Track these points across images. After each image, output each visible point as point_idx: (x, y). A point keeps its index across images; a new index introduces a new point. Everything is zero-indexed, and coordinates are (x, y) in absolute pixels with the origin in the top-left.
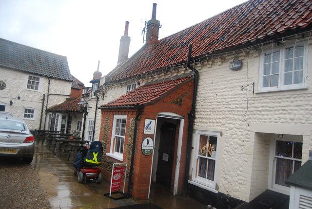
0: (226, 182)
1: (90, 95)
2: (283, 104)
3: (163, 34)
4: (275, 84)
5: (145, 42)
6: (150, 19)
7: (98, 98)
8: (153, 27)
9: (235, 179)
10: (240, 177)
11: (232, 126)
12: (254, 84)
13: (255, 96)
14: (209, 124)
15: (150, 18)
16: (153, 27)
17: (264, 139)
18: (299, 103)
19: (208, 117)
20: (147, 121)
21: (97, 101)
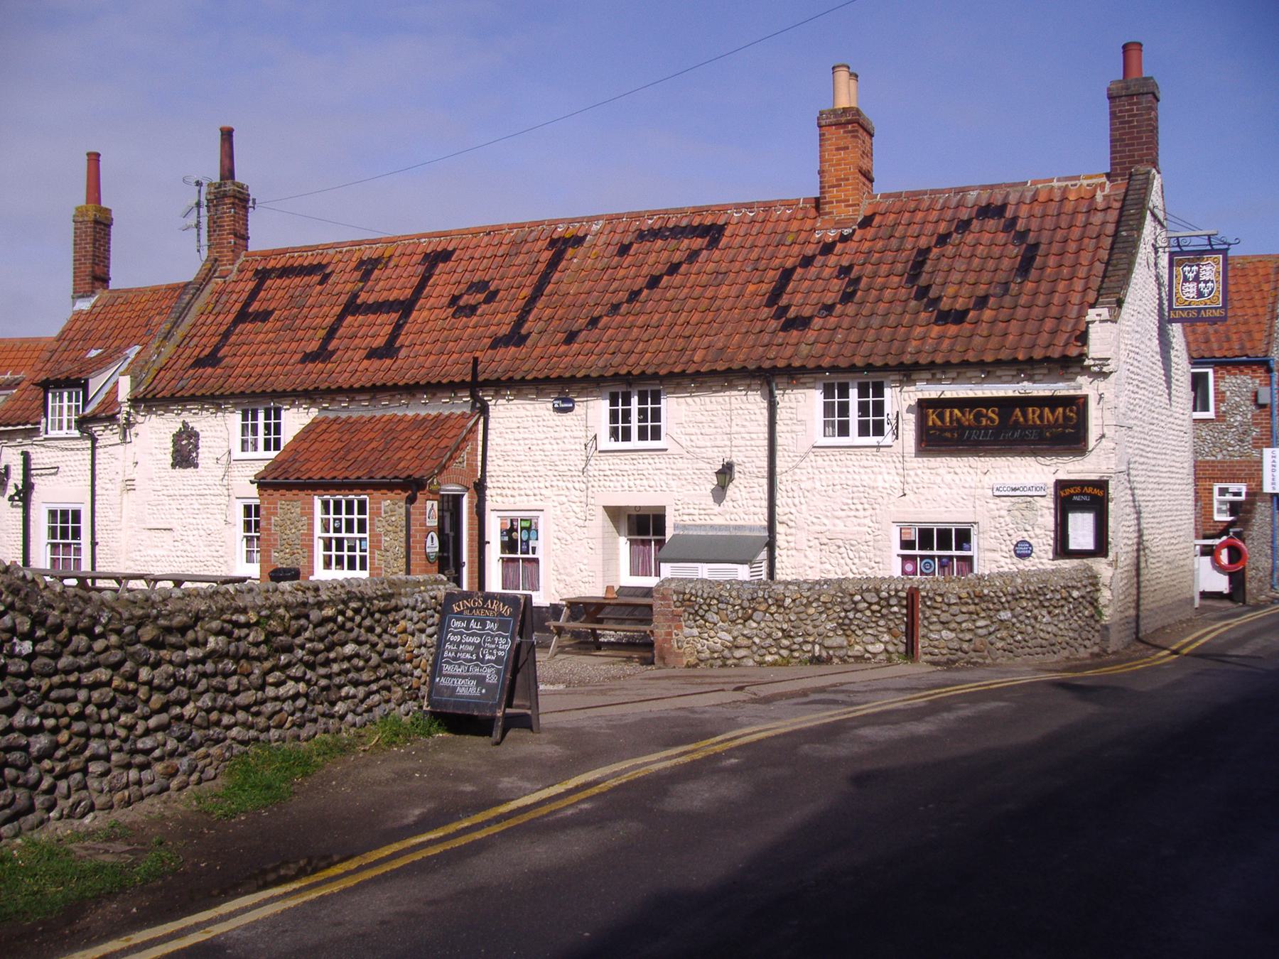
0: (562, 585)
1: (42, 427)
2: (641, 466)
3: (268, 233)
4: (627, 437)
5: (205, 253)
6: (216, 179)
7: (94, 440)
8: (228, 203)
9: (578, 577)
10: (585, 573)
11: (564, 499)
12: (595, 437)
13: (596, 453)
14: (518, 498)
15: (213, 174)
16: (228, 203)
17: (614, 513)
18: (658, 466)
19: (516, 486)
20: (429, 503)
21: (94, 448)
